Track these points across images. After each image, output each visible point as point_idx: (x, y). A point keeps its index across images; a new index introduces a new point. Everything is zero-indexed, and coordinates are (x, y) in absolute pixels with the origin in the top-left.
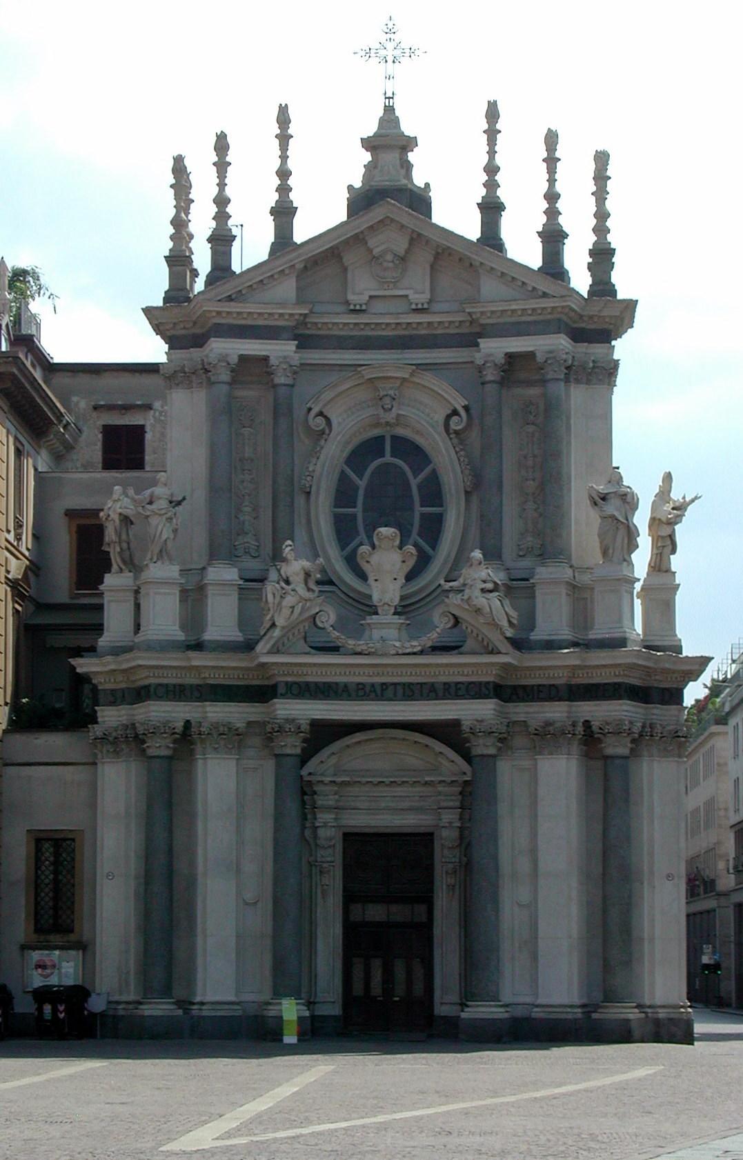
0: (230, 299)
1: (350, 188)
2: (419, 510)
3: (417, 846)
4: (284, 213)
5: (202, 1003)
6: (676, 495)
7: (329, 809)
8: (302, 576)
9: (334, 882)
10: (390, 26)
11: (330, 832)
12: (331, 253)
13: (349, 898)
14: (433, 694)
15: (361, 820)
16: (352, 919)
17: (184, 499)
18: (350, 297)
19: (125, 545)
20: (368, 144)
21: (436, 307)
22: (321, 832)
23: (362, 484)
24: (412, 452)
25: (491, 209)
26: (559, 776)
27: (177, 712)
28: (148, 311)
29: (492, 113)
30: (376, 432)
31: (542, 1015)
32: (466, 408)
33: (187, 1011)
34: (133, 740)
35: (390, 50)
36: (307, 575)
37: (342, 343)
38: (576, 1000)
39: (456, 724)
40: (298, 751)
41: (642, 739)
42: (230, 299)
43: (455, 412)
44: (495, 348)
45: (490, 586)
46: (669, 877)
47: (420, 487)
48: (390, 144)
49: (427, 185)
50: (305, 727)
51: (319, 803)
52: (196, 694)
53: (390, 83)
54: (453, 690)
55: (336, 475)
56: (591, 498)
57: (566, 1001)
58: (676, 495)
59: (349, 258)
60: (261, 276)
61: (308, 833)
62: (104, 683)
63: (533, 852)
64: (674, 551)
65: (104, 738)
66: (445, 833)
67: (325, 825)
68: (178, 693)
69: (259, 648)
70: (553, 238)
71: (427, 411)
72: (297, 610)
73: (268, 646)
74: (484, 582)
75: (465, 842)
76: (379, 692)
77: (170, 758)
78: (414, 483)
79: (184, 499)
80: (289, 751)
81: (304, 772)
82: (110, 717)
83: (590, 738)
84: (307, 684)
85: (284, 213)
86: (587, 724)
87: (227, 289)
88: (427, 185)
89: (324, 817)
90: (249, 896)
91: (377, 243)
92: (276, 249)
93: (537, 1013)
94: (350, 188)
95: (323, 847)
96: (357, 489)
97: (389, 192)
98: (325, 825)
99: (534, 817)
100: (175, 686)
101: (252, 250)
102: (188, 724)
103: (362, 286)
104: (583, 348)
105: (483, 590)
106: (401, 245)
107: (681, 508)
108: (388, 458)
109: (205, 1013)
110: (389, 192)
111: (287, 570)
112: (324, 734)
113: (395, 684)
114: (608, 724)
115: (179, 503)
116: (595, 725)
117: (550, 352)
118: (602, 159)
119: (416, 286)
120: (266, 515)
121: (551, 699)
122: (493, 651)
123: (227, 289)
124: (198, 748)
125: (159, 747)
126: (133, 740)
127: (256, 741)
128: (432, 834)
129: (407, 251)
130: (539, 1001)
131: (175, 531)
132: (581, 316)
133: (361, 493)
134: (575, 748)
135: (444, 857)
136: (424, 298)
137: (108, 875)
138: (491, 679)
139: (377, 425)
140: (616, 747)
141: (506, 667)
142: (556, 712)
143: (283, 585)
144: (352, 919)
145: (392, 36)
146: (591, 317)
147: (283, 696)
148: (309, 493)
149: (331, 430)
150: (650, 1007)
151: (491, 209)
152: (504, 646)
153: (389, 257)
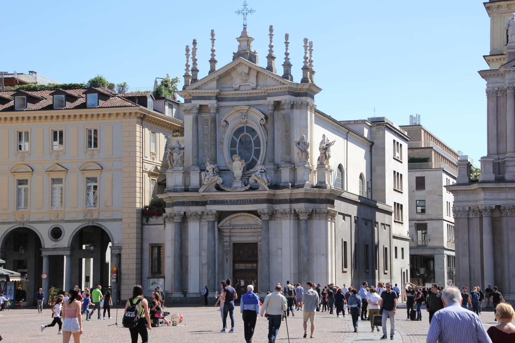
0: (196, 89)
1: (234, 53)
2: (254, 148)
3: (254, 246)
4: (213, 61)
7: (227, 236)
8: (212, 169)
9: (230, 257)
12: (228, 72)
13: (235, 262)
15: (237, 239)
16: (236, 268)
18: (234, 86)
20: (238, 40)
21: (259, 88)
22: (225, 244)
23: (238, 141)
24: (252, 131)
25: (271, 58)
27: (182, 209)
29: (271, 29)
30: (242, 125)
33: (185, 296)
34: (171, 217)
36: (214, 169)
37: (232, 99)
42: (196, 89)
43: (262, 119)
44: (271, 100)
45: (263, 171)
47: (254, 141)
48: (245, 39)
55: (231, 139)
60: (206, 81)
62: (167, 201)
65: (166, 217)
68: (183, 204)
69: (199, 191)
70: (287, 65)
71: (255, 119)
77: (180, 223)
78: (252, 140)
82: (168, 210)
83: (296, 215)
84: (216, 200)
85: (213, 61)
86: (295, 210)
87: (195, 85)
91: (240, 69)
92: (210, 72)
94: (234, 53)
96: (236, 142)
97: (245, 54)
98: (226, 242)
101: (203, 73)
102: (185, 213)
103: (237, 81)
104: (298, 98)
105: (261, 172)
107: (328, 145)
108: (245, 133)
110: (245, 54)
112: (221, 216)
116: (297, 210)
119: (252, 81)
121: (285, 203)
122: (266, 190)
123: (195, 85)
124: (189, 220)
125: (178, 219)
126: (171, 217)
129: (249, 72)
134: (292, 218)
136: (255, 85)
138: (265, 198)
139: (241, 123)
141: (268, 194)
142: (286, 207)
144: (236, 268)
146: (300, 89)
151: (271, 58)
152: (267, 189)
153: (244, 74)
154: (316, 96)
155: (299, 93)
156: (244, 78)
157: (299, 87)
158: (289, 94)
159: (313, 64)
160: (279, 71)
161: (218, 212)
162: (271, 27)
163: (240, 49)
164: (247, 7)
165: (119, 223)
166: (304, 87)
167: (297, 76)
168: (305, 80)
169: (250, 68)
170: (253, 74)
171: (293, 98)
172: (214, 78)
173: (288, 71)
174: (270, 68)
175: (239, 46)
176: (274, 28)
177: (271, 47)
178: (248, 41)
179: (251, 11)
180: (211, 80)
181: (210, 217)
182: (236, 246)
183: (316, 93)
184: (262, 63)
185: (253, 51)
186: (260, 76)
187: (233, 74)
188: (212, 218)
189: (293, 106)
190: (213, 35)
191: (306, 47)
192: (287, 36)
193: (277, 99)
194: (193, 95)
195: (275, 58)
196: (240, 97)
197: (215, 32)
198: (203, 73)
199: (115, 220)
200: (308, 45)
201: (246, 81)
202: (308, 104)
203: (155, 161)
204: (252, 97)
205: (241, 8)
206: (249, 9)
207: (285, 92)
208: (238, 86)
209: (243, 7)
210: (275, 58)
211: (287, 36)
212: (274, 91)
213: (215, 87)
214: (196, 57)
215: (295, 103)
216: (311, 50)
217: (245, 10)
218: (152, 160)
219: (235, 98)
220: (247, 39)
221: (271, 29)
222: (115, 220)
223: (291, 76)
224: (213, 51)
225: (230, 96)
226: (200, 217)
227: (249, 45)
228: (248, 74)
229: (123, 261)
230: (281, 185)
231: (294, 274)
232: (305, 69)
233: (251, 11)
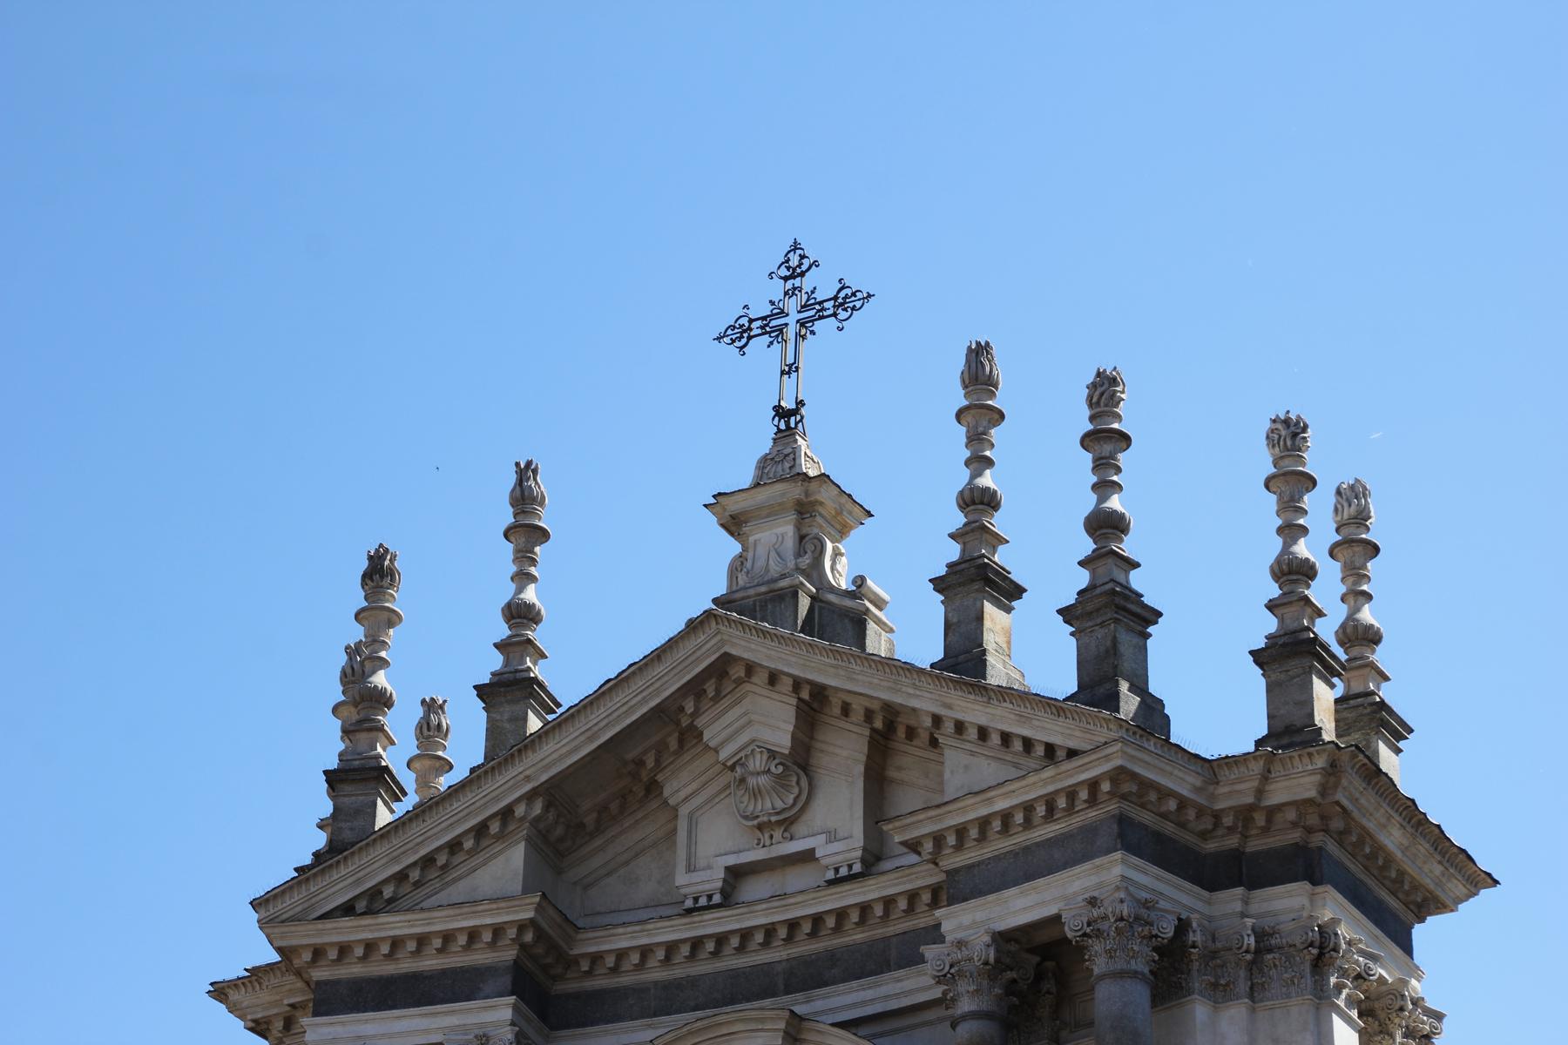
0: (348, 909)
4: (509, 690)
10: (794, 261)
20: (734, 517)
42: (348, 909)
44: (971, 924)
104: (1231, 900)
106: (772, 721)
119: (835, 820)
132: (1217, 816)
145: (797, 282)
146: (1245, 814)
151: (975, 580)
153: (757, 762)
154: (1427, 934)
155: (1236, 856)
156: (768, 805)
157: (1235, 794)
158: (1131, 848)
159: (1381, 656)
160: (1034, 651)
162: (978, 354)
163: (742, 579)
164: (807, 283)
166: (1279, 794)
167: (1212, 700)
168: (1289, 731)
169: (814, 706)
170: (844, 753)
171: (1178, 897)
172: (506, 814)
173: (1113, 650)
174: (964, 658)
176: (1002, 367)
177: (978, 502)
178: (804, 510)
179: (846, 302)
180: (481, 830)
183: (1428, 904)
184: (911, 630)
185: (844, 584)
186: (908, 763)
187: (679, 785)
189: (1173, 967)
190: (524, 498)
191: (1290, 483)
192: (1104, 392)
193: (1020, 906)
194: (319, 974)
195: (1017, 591)
196: (734, 974)
201: (787, 823)
202: (1323, 950)
204: (831, 957)
205: (762, 294)
207: (1089, 831)
208: (713, 879)
209: (777, 289)
210: (1017, 591)
211: (1104, 392)
212: (999, 845)
213: (517, 887)
214: (357, 633)
215: (1195, 937)
216: (1356, 548)
219: (693, 982)
220: (795, 491)
221: (978, 371)
223: (1140, 688)
224: (520, 615)
225: (656, 973)
227: (809, 547)
228: (801, 761)
232: (1288, 655)
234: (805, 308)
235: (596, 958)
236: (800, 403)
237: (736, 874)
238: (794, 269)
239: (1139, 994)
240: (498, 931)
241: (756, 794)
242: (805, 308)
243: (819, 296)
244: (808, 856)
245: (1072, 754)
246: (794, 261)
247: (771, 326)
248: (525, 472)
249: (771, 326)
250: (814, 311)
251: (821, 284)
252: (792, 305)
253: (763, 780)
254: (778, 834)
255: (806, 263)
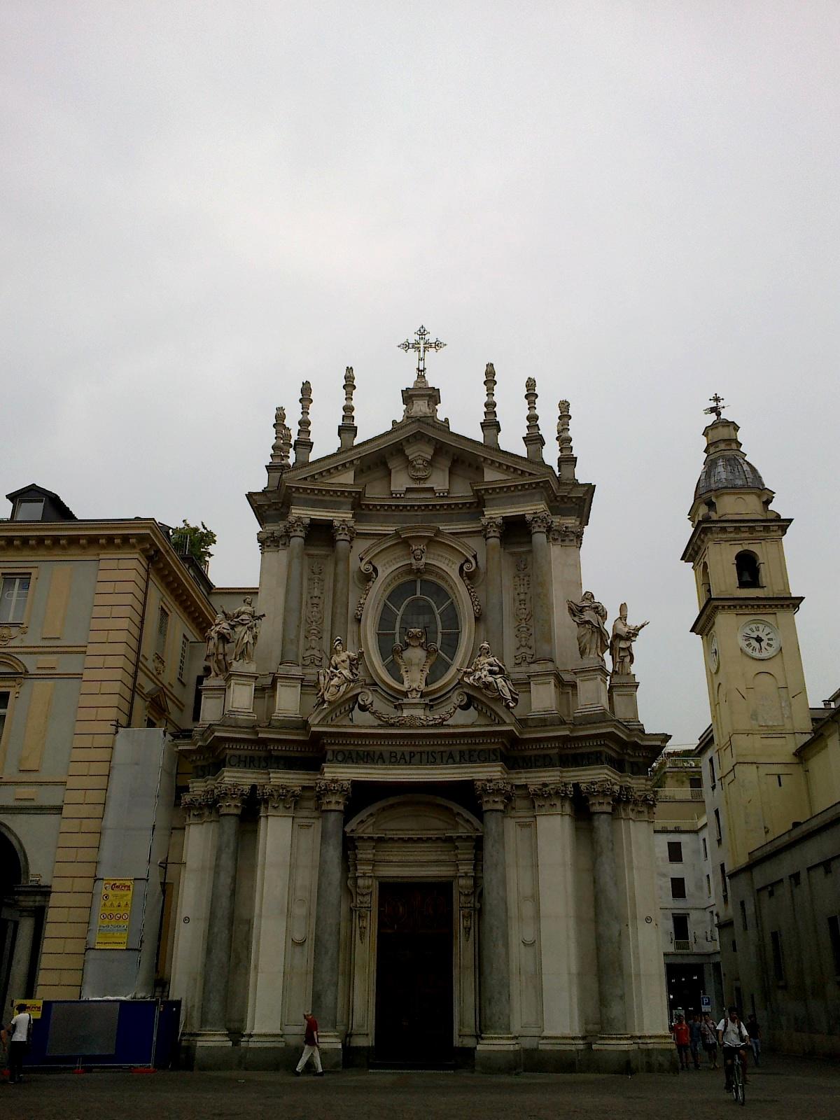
0: (305, 479)
1: (394, 422)
4: (347, 429)
5: (251, 1036)
6: (632, 621)
7: (368, 862)
10: (422, 331)
11: (368, 882)
14: (451, 760)
17: (264, 615)
19: (221, 657)
22: (360, 882)
23: (400, 613)
25: (491, 425)
26: (555, 830)
28: (250, 496)
30: (411, 577)
31: (548, 1047)
32: (475, 557)
33: (236, 1043)
35: (422, 343)
38: (577, 1032)
39: (470, 783)
40: (341, 807)
41: (621, 801)
44: (496, 513)
45: (496, 669)
46: (648, 920)
48: (421, 395)
49: (447, 420)
50: (346, 785)
51: (359, 856)
52: (263, 764)
53: (422, 363)
54: (467, 757)
56: (570, 609)
57: (567, 1032)
58: (632, 621)
59: (394, 464)
61: (350, 882)
63: (535, 898)
64: (632, 661)
66: (462, 882)
67: (364, 876)
70: (534, 439)
72: (343, 689)
73: (319, 719)
74: (491, 665)
75: (478, 891)
76: (408, 758)
79: (264, 615)
80: (333, 807)
81: (348, 829)
85: (347, 429)
86: (576, 786)
88: (447, 420)
89: (363, 869)
90: (298, 937)
93: (545, 1046)
94: (394, 422)
95: (363, 895)
98: (364, 876)
99: (535, 866)
100: (246, 757)
102: (254, 787)
106: (428, 452)
109: (251, 1045)
111: (336, 659)
112: (362, 795)
113: (421, 753)
114: (592, 783)
115: (259, 618)
116: (583, 786)
117: (535, 513)
118: (564, 406)
120: (326, 636)
125: (231, 807)
127: (311, 804)
128: (451, 883)
130: (545, 1034)
131: (255, 638)
132: (556, 497)
133: (399, 618)
134: (568, 809)
135: (459, 901)
137: (185, 919)
140: (600, 806)
142: (551, 776)
143: (332, 669)
145: (423, 336)
147: (330, 761)
148: (359, 621)
149: (377, 576)
150: (640, 1038)
156: (420, 474)
161: (356, 784)
165: (54, 818)
175: (406, 411)
179: (438, 345)
180: (344, 465)
181: (333, 799)
182: (391, 891)
188: (336, 803)
197: (355, 373)
198: (325, 443)
199: (40, 810)
200: (565, 417)
203: (159, 677)
205: (413, 338)
206: (432, 340)
217: (422, 342)
218: (155, 673)
222: (40, 810)
226: (293, 801)
229: (49, 930)
230: (531, 715)
231: (580, 975)
233: (438, 345)
234: (426, 343)
235: (368, 505)
236: (425, 369)
237: (409, 490)
238: (422, 333)
239: (544, 536)
240: (350, 493)
241: (419, 470)
242: (426, 343)
243: (430, 341)
244: (431, 490)
245: (530, 474)
246: (422, 331)
247: (415, 346)
248: (350, 370)
249: (415, 346)
250: (428, 345)
251: (431, 338)
252: (422, 342)
253: (421, 466)
254: (422, 482)
255: (426, 332)
